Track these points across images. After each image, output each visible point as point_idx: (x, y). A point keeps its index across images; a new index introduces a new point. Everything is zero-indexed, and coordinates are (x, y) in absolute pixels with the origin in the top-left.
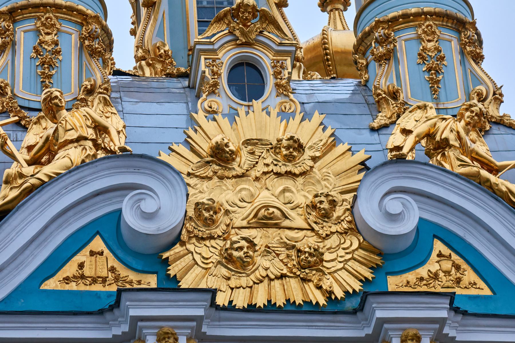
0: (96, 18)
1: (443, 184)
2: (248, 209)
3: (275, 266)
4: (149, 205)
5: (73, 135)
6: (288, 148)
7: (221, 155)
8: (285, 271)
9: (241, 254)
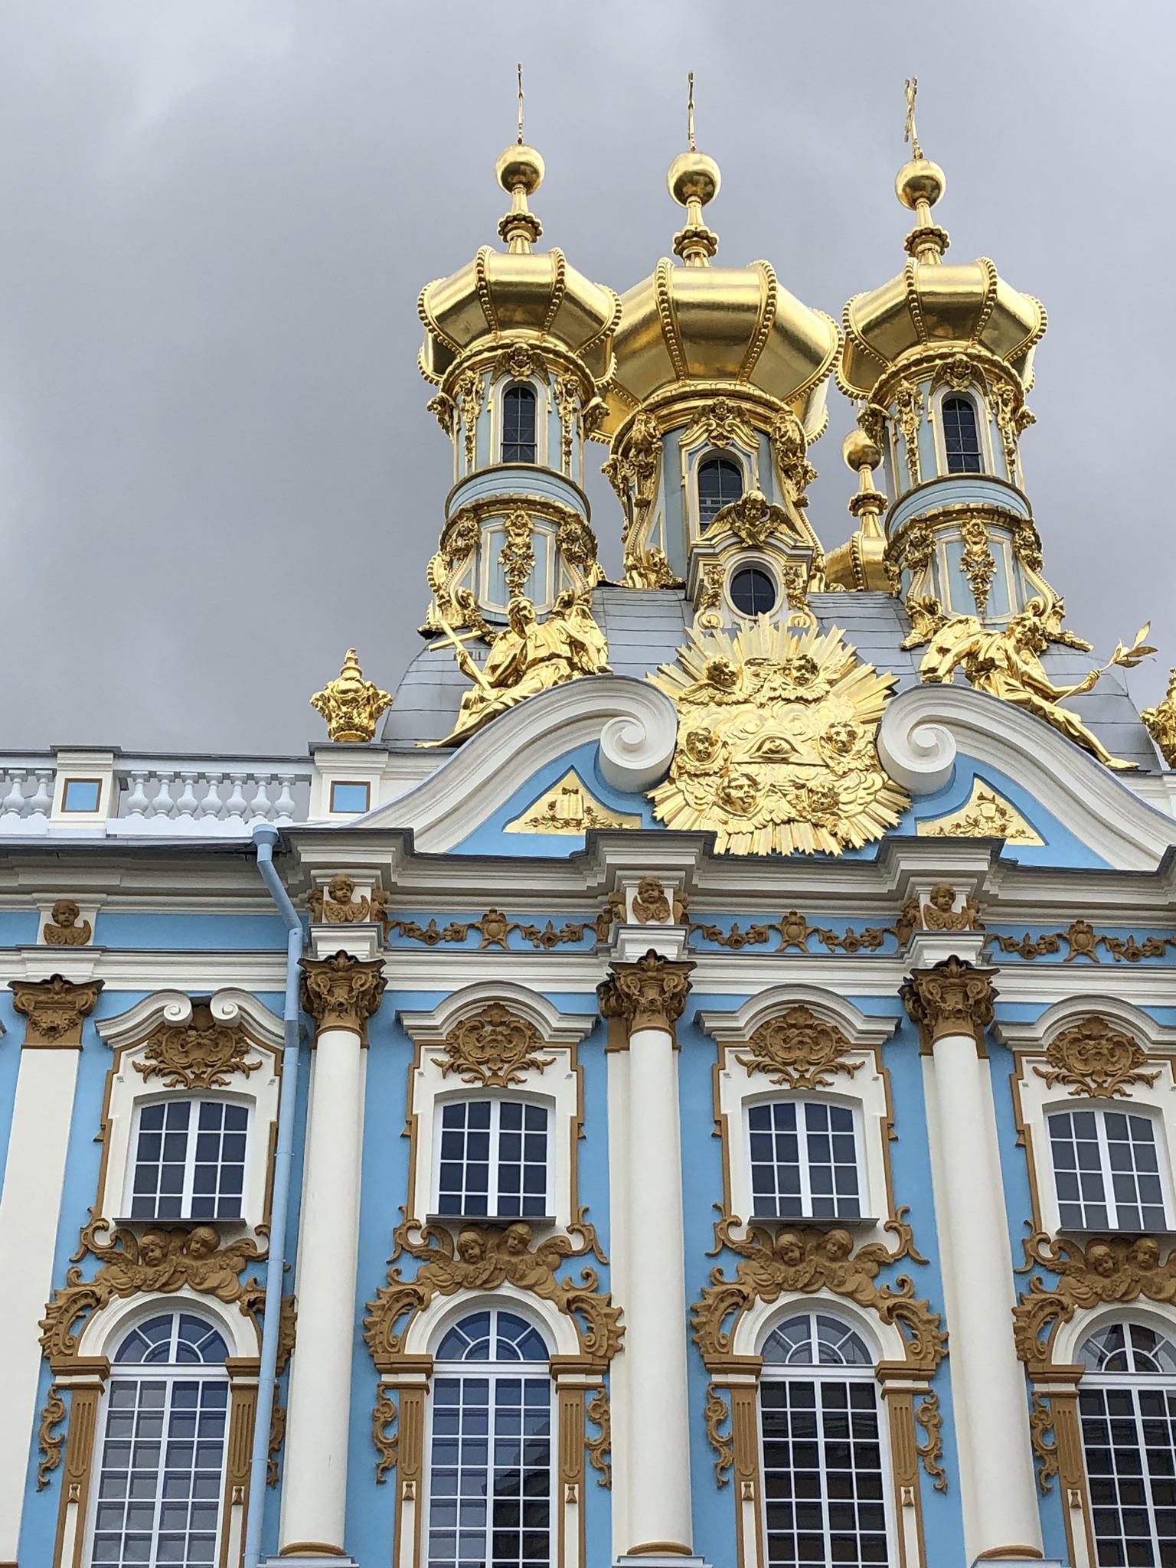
0: (577, 516)
1: (985, 712)
2: (753, 742)
3: (784, 809)
4: (631, 734)
5: (543, 653)
6: (799, 669)
7: (720, 677)
8: (794, 814)
9: (741, 794)
